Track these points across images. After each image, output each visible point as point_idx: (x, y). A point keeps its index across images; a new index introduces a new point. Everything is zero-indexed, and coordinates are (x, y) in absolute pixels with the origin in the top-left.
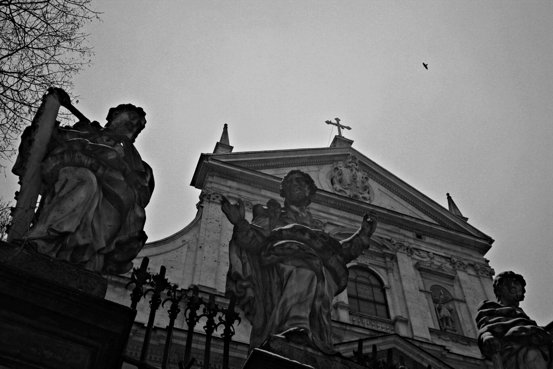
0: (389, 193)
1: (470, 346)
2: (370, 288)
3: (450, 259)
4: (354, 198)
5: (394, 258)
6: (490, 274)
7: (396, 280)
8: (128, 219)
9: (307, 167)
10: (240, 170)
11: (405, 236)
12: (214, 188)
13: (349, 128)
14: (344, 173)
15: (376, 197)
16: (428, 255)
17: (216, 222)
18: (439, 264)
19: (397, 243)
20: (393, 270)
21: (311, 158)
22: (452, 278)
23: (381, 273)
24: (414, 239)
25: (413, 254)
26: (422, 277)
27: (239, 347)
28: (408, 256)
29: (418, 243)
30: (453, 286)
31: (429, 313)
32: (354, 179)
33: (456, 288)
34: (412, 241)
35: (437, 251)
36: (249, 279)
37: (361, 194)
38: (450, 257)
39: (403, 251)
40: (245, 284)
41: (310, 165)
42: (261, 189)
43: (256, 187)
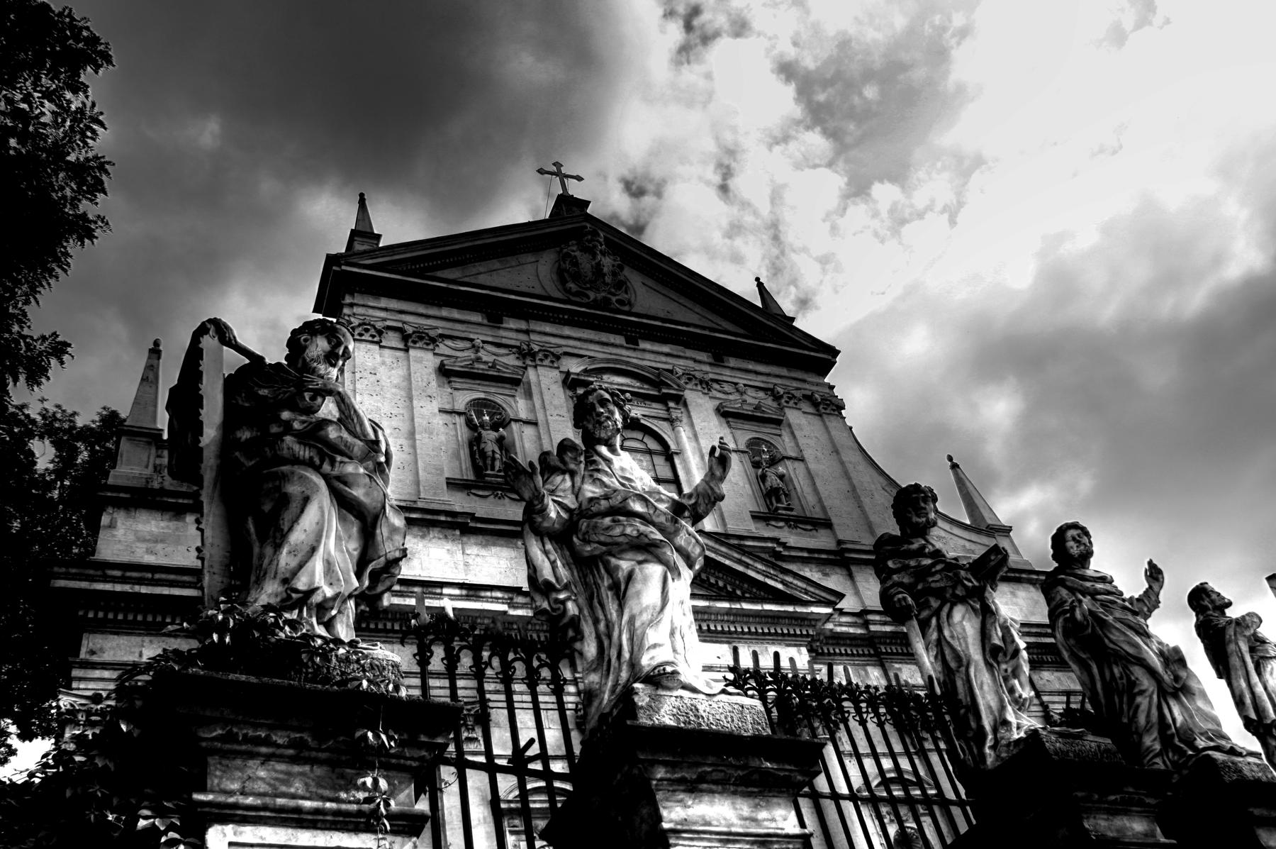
0: (659, 288)
1: (817, 530)
2: (648, 457)
3: (772, 390)
4: (604, 304)
5: (679, 400)
8: (378, 531)
12: (358, 315)
13: (579, 179)
17: (370, 375)
18: (756, 402)
19: (683, 374)
24: (710, 364)
26: (730, 427)
27: (446, 591)
29: (718, 370)
30: (780, 435)
33: (786, 437)
34: (707, 368)
35: (750, 380)
36: (566, 587)
37: (614, 295)
38: (771, 386)
40: (562, 596)
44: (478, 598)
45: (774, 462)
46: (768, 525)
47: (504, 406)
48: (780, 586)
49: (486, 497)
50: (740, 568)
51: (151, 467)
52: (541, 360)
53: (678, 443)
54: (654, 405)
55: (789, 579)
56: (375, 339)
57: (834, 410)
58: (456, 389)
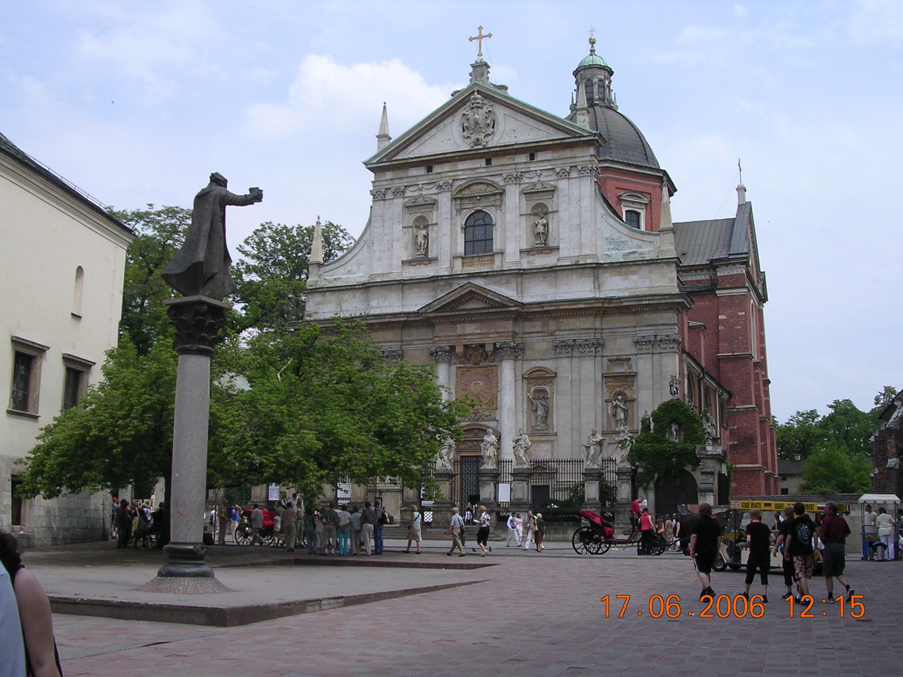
5: (502, 193)
6: (591, 170)
7: (503, 213)
9: (444, 121)
10: (388, 164)
11: (516, 164)
15: (499, 126)
20: (500, 207)
22: (553, 190)
23: (491, 211)
26: (527, 201)
27: (387, 316)
28: (516, 184)
31: (525, 234)
33: (555, 199)
34: (523, 166)
35: (544, 166)
38: (554, 167)
39: (511, 182)
42: (408, 169)
44: (397, 317)
45: (547, 213)
48: (499, 300)
49: (415, 265)
50: (484, 294)
53: (496, 220)
54: (492, 198)
58: (410, 214)
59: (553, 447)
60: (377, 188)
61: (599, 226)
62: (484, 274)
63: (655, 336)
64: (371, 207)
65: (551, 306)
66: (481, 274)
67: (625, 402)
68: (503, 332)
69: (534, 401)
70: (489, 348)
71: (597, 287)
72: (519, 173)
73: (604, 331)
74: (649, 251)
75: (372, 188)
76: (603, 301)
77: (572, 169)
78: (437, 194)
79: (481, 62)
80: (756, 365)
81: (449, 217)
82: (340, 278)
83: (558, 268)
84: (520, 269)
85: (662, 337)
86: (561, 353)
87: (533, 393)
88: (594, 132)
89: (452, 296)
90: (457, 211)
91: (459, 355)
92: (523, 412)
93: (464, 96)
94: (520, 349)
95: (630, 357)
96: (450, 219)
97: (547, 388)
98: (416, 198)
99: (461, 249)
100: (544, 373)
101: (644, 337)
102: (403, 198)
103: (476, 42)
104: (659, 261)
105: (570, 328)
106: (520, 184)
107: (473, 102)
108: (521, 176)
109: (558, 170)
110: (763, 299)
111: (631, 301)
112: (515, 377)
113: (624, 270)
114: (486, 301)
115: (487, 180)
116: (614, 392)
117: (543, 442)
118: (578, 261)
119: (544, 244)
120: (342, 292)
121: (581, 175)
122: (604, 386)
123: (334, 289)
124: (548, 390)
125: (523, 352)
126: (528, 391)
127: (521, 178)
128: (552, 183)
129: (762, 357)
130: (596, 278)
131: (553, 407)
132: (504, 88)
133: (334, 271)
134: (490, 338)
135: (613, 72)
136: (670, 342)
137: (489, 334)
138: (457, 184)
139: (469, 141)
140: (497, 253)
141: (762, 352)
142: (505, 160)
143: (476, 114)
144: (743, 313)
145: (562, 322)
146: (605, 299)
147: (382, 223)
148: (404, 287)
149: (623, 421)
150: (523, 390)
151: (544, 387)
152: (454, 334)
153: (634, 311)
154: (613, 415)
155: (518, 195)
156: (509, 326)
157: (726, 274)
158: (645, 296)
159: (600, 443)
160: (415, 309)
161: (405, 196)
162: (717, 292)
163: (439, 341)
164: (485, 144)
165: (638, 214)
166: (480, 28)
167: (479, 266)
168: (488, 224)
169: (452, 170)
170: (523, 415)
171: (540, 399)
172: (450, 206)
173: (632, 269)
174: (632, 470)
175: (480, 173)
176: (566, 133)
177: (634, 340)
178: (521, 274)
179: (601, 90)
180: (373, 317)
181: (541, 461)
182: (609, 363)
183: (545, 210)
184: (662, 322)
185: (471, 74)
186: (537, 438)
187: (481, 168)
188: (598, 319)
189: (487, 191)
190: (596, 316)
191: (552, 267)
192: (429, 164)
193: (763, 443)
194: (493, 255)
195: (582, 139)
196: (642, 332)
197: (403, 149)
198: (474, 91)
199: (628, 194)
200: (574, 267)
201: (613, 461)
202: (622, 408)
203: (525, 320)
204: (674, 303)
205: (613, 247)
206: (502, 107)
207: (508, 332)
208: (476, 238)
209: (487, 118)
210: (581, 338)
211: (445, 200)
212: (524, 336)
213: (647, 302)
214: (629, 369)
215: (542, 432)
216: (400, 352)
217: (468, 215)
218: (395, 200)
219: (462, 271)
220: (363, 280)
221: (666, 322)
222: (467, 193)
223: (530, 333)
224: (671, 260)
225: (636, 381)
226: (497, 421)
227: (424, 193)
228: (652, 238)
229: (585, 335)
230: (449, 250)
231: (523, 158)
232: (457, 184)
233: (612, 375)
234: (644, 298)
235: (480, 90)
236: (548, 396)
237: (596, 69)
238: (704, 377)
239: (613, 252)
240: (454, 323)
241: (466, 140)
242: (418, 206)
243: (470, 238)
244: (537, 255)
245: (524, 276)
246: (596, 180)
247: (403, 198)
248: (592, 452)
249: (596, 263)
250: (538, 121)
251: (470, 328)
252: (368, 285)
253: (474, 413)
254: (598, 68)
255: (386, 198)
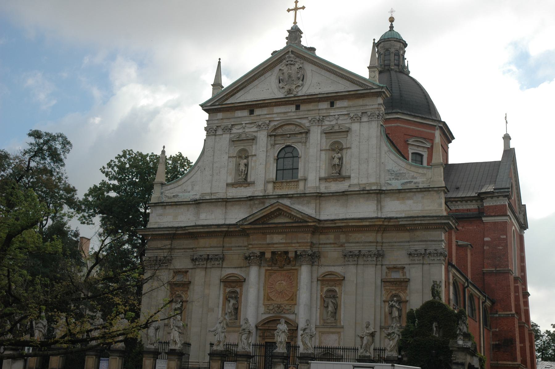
5: (307, 133)
6: (378, 116)
7: (308, 148)
10: (220, 106)
11: (319, 110)
14: (285, 71)
16: (335, 118)
20: (306, 142)
21: (264, 69)
22: (348, 131)
23: (299, 147)
25: (325, 121)
26: (327, 139)
27: (212, 227)
28: (318, 126)
29: (328, 111)
31: (324, 165)
32: (290, 76)
33: (349, 138)
34: (325, 111)
35: (342, 112)
38: (349, 113)
39: (315, 124)
41: (266, 73)
42: (235, 111)
43: (232, 111)
44: (220, 228)
45: (342, 149)
46: (326, 182)
47: (248, 150)
48: (300, 217)
50: (289, 212)
51: (160, 193)
52: (262, 128)
54: (299, 136)
55: (303, 214)
56: (214, 134)
57: (375, 118)
59: (339, 338)
60: (210, 125)
61: (383, 161)
62: (289, 196)
63: (425, 250)
64: (205, 140)
65: (342, 223)
66: (287, 196)
67: (399, 303)
68: (303, 242)
69: (326, 300)
70: (291, 255)
71: (379, 208)
72: (321, 117)
73: (384, 245)
74: (423, 182)
75: (206, 126)
76: (383, 220)
77: (363, 115)
78: (257, 131)
79: (295, 29)
80: (516, 279)
81: (265, 150)
82: (178, 195)
83: (348, 193)
84: (318, 193)
85: (431, 251)
86: (349, 261)
87: (325, 292)
88: (382, 85)
89: (264, 212)
90: (271, 145)
91: (268, 260)
92: (316, 308)
93: (280, 56)
94: (317, 257)
95: (405, 266)
96: (265, 152)
97: (337, 289)
98: (240, 135)
99: (273, 176)
100: (334, 276)
101: (416, 250)
102: (230, 134)
103: (292, 13)
104: (430, 189)
105: (357, 241)
106: (322, 126)
107: (287, 60)
108: (323, 119)
109: (352, 115)
110: (524, 226)
111: (406, 221)
112: (312, 279)
113: (401, 195)
114: (291, 217)
115: (296, 122)
116: (391, 294)
117: (333, 333)
118: (365, 188)
119: (339, 174)
120: (178, 207)
121: (370, 120)
122: (383, 288)
123: (173, 204)
124: (337, 290)
125: (319, 259)
126: (322, 291)
127: (323, 120)
128: (347, 125)
129: (523, 274)
130: (379, 202)
131: (340, 306)
132: (313, 49)
133: (173, 190)
134: (292, 247)
135: (407, 45)
136: (437, 255)
137: (292, 243)
138: (272, 124)
139: (283, 91)
140: (301, 180)
141: (523, 269)
142: (311, 106)
143: (289, 69)
144: (505, 237)
145: (351, 236)
146: (385, 218)
147: (213, 153)
148: (227, 204)
149: (397, 318)
150: (317, 290)
151: (334, 288)
152: (265, 242)
153: (408, 229)
154: (389, 313)
155: (319, 135)
156: (307, 237)
157: (491, 204)
158: (418, 217)
159: (372, 335)
160: (234, 222)
161: (232, 132)
162: (483, 219)
163: (252, 248)
164: (295, 93)
165: (422, 156)
166: (296, 2)
167: (287, 189)
168: (295, 156)
169: (268, 113)
170: (316, 310)
171: (331, 298)
172: (266, 142)
173: (409, 195)
174: (399, 359)
175: (291, 116)
176: (360, 86)
177: (408, 252)
178: (319, 196)
179: (397, 57)
180: (201, 227)
181: (330, 348)
182: (387, 270)
183: (340, 147)
184: (431, 239)
185: (287, 38)
186: (327, 330)
187: (291, 112)
188: (379, 235)
189: (296, 130)
190: (378, 231)
191: (343, 192)
192: (251, 108)
193: (522, 345)
194: (298, 181)
195: (372, 91)
196: (415, 246)
197: (232, 96)
198: (289, 52)
199: (414, 140)
200: (362, 192)
201: (382, 350)
202: (396, 308)
203: (321, 233)
204: (441, 223)
205: (393, 177)
206: (310, 64)
207: (307, 242)
208: (285, 167)
209: (298, 73)
210: (365, 249)
211: (262, 137)
212: (320, 246)
213: (419, 222)
214: (403, 276)
215: (332, 324)
216: (221, 256)
217: (280, 149)
218: (224, 136)
219: (273, 193)
220: (196, 198)
221: (435, 239)
222: (280, 131)
223: (325, 244)
224: (439, 189)
225: (409, 286)
226: (296, 314)
227: (246, 130)
228: (425, 171)
229: (368, 247)
230: (264, 176)
231: (325, 105)
232: (272, 124)
233: (389, 280)
234: (417, 219)
235: (293, 50)
236: (338, 296)
237: (393, 42)
238: (468, 286)
239: (393, 181)
240: (265, 234)
241: (281, 90)
242: (242, 140)
243: (281, 167)
244: (332, 182)
245: (322, 198)
246: (382, 124)
247: (230, 134)
248: (365, 342)
249: (379, 190)
250: (339, 76)
251: (277, 239)
252: (199, 201)
253: (277, 307)
254: (395, 41)
255: (217, 134)
